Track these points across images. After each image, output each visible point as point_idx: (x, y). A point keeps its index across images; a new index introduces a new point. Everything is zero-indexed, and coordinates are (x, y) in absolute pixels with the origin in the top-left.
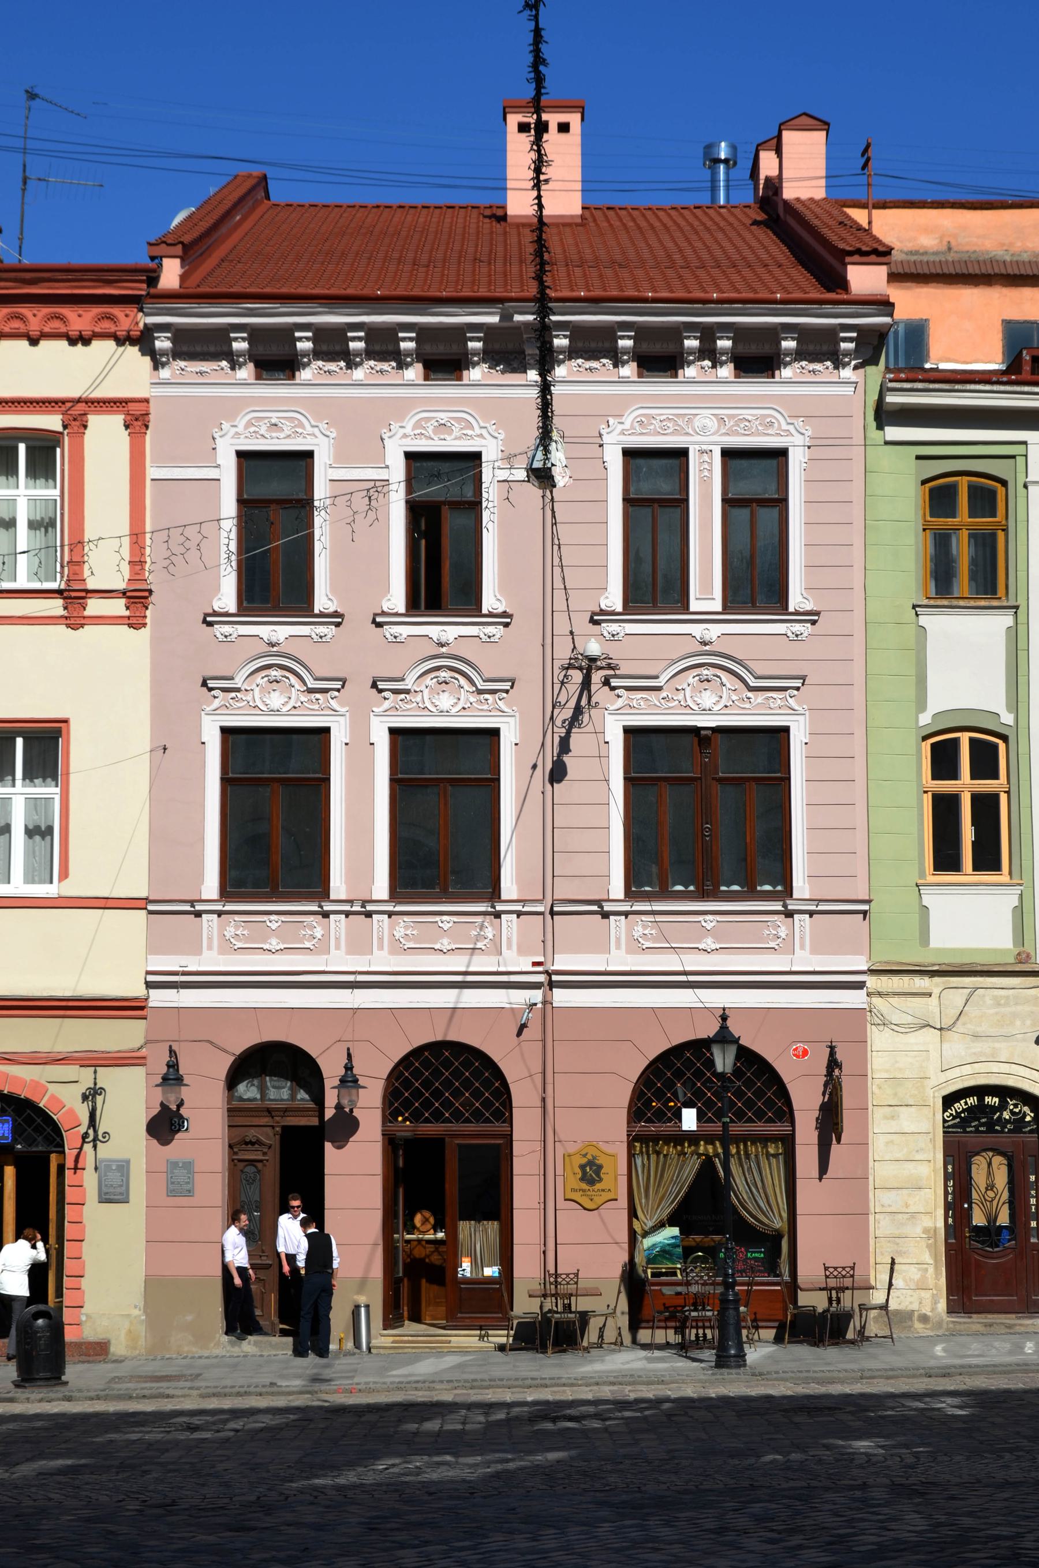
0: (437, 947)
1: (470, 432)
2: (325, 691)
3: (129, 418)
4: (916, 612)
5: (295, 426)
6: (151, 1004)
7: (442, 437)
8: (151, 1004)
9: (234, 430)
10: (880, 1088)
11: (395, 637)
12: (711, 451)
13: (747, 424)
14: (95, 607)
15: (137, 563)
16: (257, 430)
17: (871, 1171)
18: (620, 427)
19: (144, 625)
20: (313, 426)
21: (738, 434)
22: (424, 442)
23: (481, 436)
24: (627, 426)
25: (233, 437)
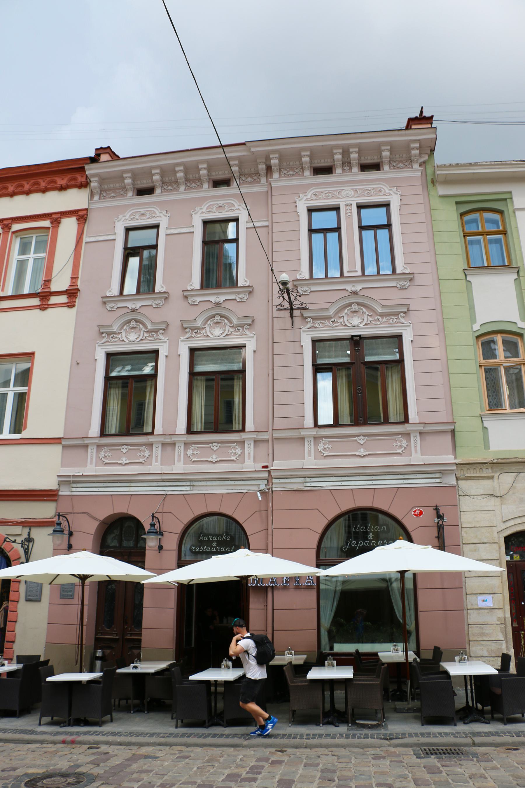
0: (209, 460)
1: (233, 208)
2: (156, 331)
3: (78, 217)
4: (465, 274)
5: (152, 213)
6: (60, 493)
7: (220, 211)
8: (60, 493)
9: (124, 218)
10: (466, 533)
11: (194, 302)
12: (351, 204)
13: (369, 191)
14: (54, 300)
15: (74, 278)
16: (134, 217)
17: (463, 583)
18: (305, 198)
19: (74, 306)
20: (160, 213)
21: (365, 196)
22: (211, 214)
23: (238, 209)
24: (309, 196)
25: (123, 221)
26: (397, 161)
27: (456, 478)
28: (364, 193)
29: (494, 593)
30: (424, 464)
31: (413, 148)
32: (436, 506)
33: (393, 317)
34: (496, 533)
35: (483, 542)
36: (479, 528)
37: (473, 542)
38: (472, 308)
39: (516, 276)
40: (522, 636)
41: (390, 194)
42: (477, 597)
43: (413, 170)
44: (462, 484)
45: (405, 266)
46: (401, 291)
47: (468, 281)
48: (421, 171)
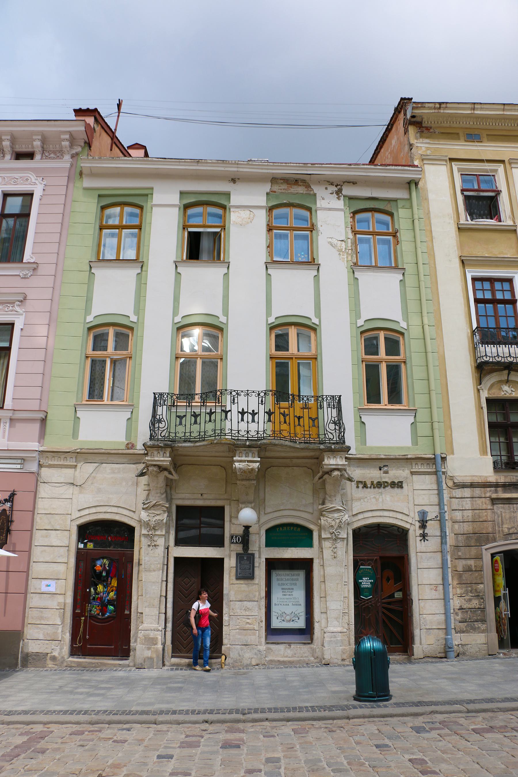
4: (90, 266)
10: (41, 519)
13: (16, 180)
21: (11, 184)
26: (50, 151)
27: (39, 464)
28: (11, 181)
29: (58, 579)
30: (8, 450)
31: (63, 140)
32: (14, 491)
33: (9, 305)
34: (69, 522)
35: (55, 528)
36: (54, 515)
37: (46, 528)
38: (89, 300)
39: (139, 271)
40: (82, 621)
41: (35, 184)
42: (41, 582)
43: (63, 161)
44: (44, 471)
45: (32, 256)
46: (23, 279)
47: (92, 273)
48: (70, 162)
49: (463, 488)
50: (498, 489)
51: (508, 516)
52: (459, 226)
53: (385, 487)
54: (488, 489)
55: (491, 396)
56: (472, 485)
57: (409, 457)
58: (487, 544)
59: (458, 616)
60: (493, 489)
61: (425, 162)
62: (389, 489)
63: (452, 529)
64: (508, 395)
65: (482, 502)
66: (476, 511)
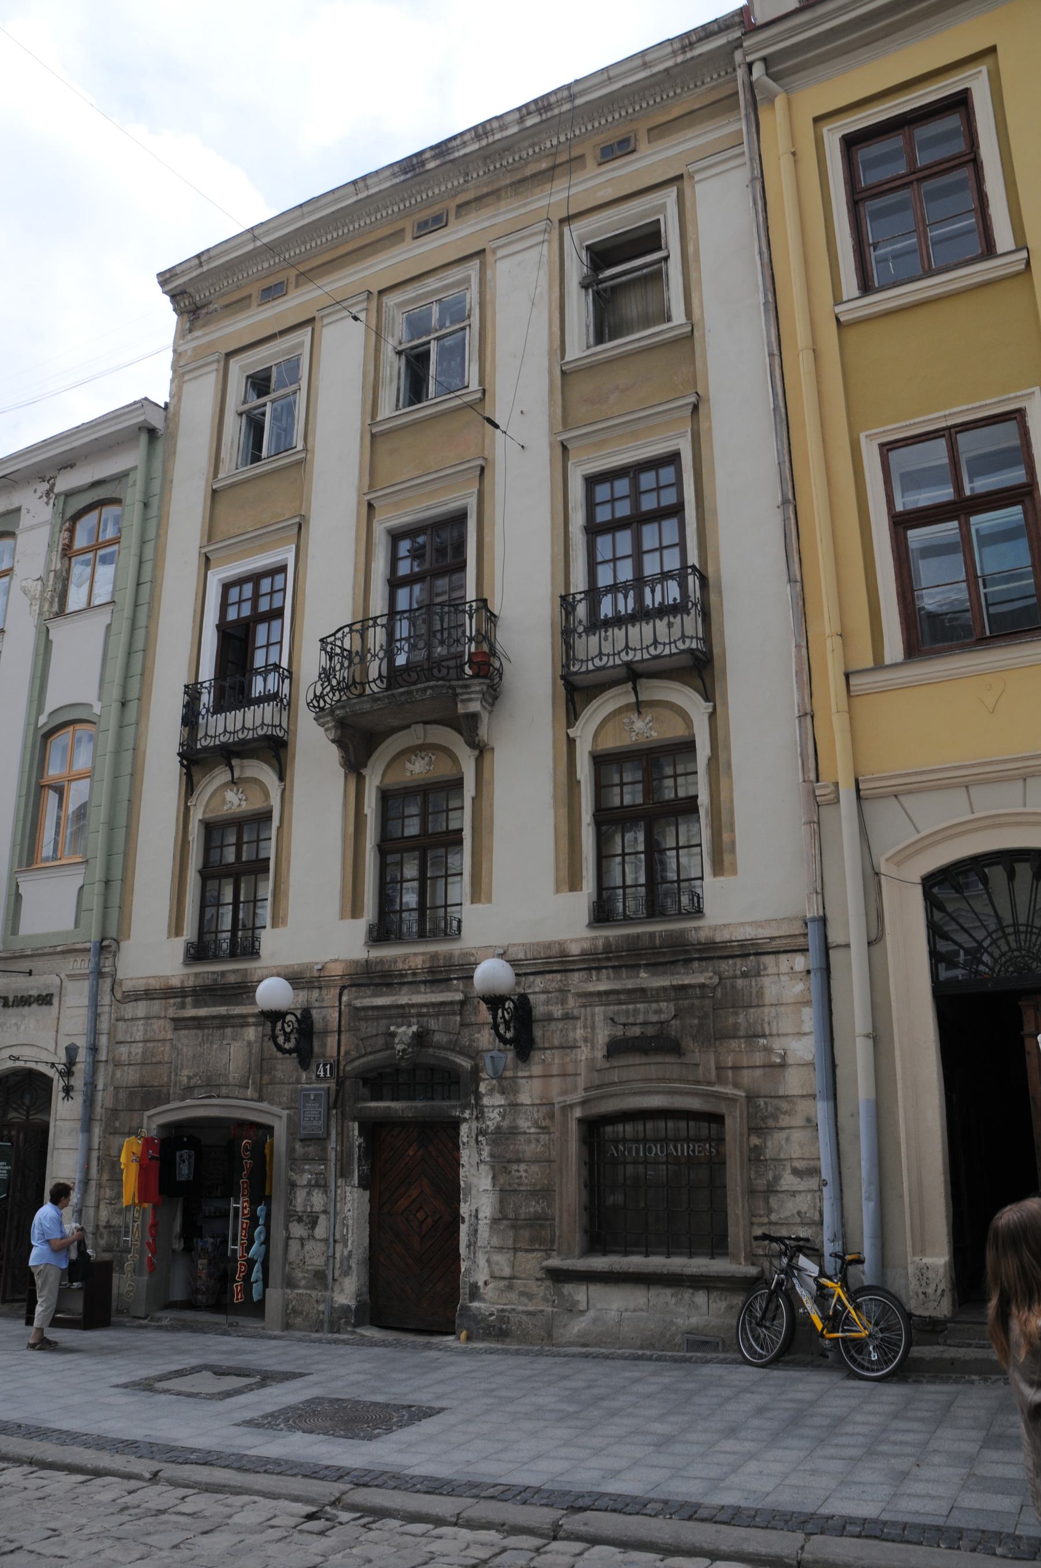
49: (136, 1000)
50: (189, 1000)
51: (190, 1054)
52: (214, 487)
53: (30, 1005)
54: (172, 1001)
55: (207, 816)
56: (148, 994)
57: (59, 949)
58: (156, 1107)
59: (102, 1238)
60: (179, 1000)
61: (187, 378)
62: (34, 1006)
63: (112, 1077)
64: (235, 809)
65: (160, 1027)
66: (149, 1045)
